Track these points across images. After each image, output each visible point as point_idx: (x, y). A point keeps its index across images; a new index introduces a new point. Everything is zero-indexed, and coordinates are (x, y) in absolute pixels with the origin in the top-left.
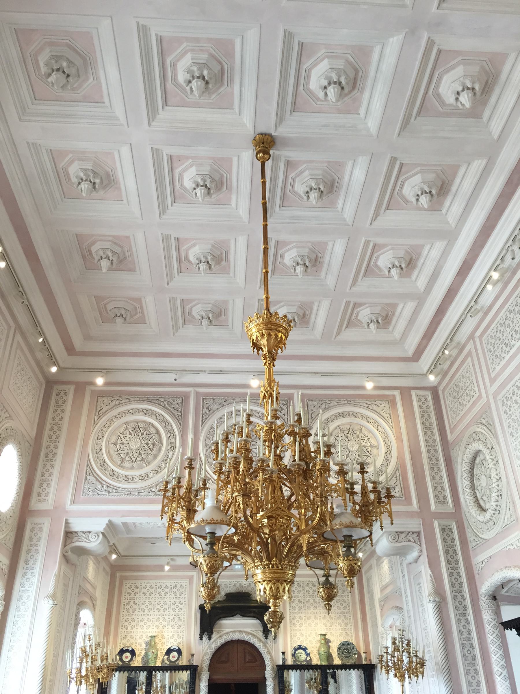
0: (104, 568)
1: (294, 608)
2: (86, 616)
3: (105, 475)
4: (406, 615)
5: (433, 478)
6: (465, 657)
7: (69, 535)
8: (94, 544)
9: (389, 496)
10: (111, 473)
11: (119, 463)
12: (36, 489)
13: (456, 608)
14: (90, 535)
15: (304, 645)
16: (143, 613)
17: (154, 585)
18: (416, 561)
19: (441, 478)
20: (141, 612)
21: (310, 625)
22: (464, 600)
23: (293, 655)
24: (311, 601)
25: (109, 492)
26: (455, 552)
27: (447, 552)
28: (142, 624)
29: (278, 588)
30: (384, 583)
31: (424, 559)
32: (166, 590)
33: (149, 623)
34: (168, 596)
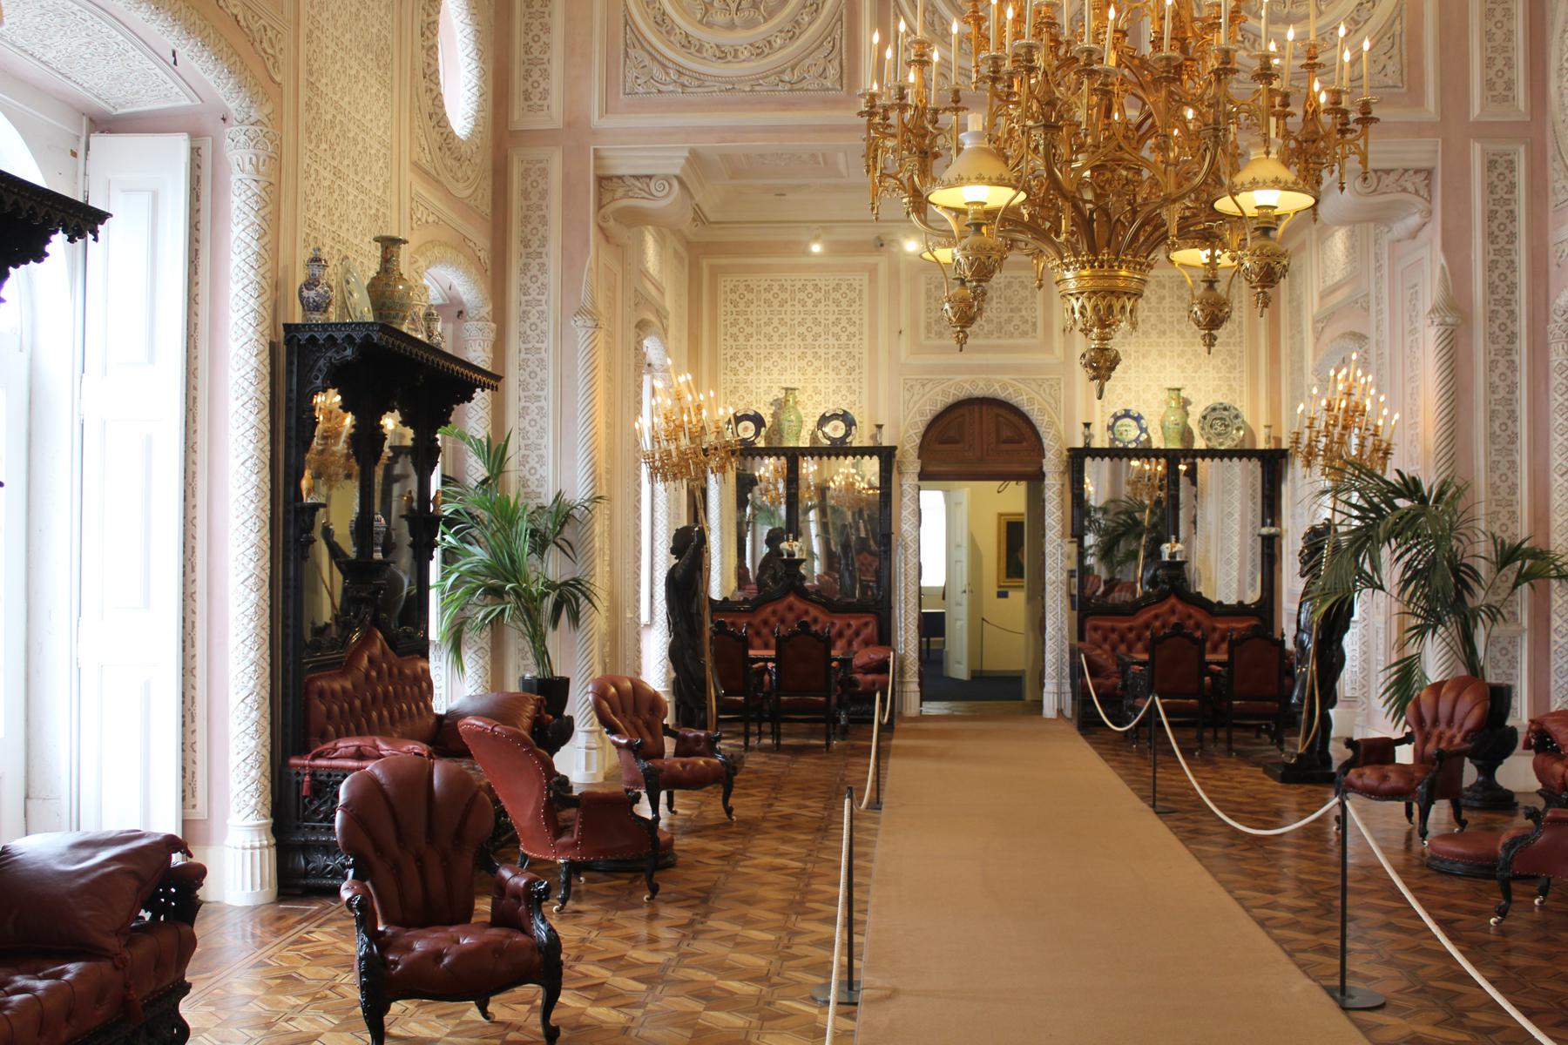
0: (676, 251)
2: (652, 348)
4: (1373, 350)
5: (1488, 35)
6: (1492, 437)
7: (604, 183)
8: (664, 201)
9: (1366, 119)
12: (518, 85)
13: (1492, 338)
14: (652, 184)
17: (787, 285)
18: (1413, 235)
19: (1509, 36)
20: (764, 342)
22: (1514, 321)
23: (1111, 428)
24: (1153, 319)
25: (683, 85)
26: (1511, 216)
27: (1491, 216)
28: (769, 364)
29: (1110, 307)
30: (1329, 283)
31: (1434, 231)
32: (817, 296)
33: (782, 364)
34: (821, 307)
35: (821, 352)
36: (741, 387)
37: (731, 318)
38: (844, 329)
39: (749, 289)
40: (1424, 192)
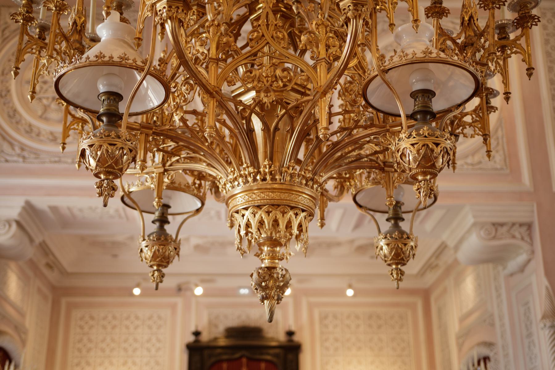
3: (17, 130)
10: (28, 129)
11: (40, 113)
40: (527, 238)
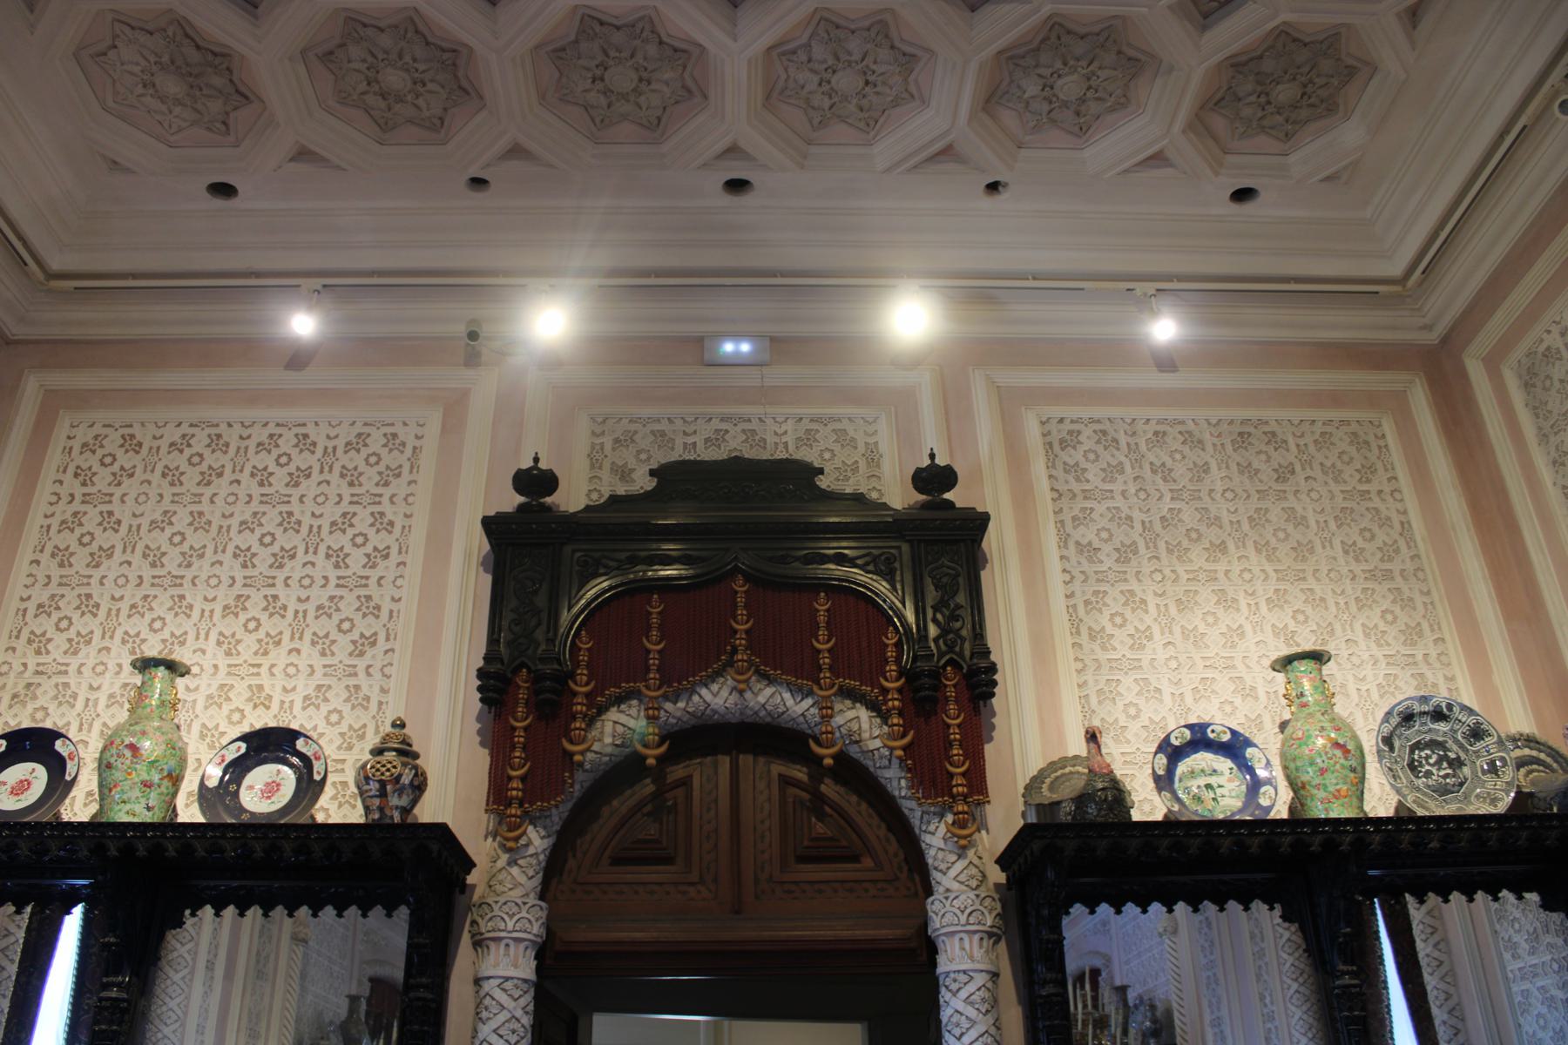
1: (1089, 551)
15: (1175, 727)
16: (147, 573)
17: (231, 436)
21: (1198, 640)
24: (1189, 516)
34: (309, 487)
35: (289, 597)
36: (48, 685)
37: (64, 511)
38: (360, 540)
39: (131, 443)
